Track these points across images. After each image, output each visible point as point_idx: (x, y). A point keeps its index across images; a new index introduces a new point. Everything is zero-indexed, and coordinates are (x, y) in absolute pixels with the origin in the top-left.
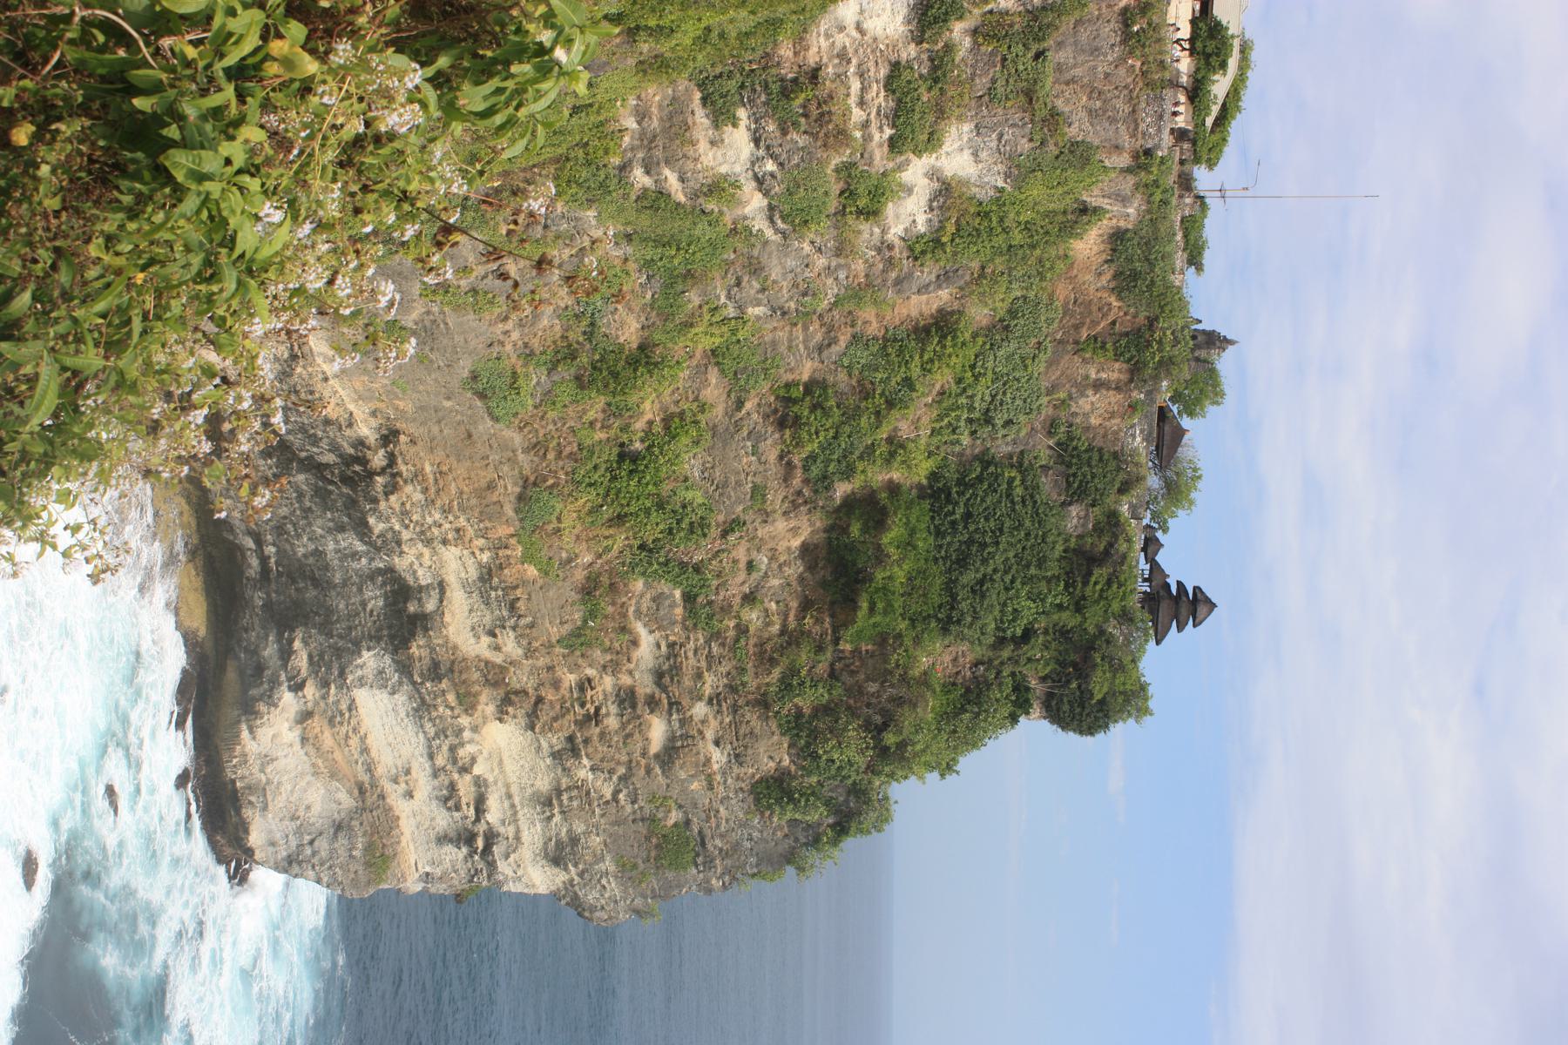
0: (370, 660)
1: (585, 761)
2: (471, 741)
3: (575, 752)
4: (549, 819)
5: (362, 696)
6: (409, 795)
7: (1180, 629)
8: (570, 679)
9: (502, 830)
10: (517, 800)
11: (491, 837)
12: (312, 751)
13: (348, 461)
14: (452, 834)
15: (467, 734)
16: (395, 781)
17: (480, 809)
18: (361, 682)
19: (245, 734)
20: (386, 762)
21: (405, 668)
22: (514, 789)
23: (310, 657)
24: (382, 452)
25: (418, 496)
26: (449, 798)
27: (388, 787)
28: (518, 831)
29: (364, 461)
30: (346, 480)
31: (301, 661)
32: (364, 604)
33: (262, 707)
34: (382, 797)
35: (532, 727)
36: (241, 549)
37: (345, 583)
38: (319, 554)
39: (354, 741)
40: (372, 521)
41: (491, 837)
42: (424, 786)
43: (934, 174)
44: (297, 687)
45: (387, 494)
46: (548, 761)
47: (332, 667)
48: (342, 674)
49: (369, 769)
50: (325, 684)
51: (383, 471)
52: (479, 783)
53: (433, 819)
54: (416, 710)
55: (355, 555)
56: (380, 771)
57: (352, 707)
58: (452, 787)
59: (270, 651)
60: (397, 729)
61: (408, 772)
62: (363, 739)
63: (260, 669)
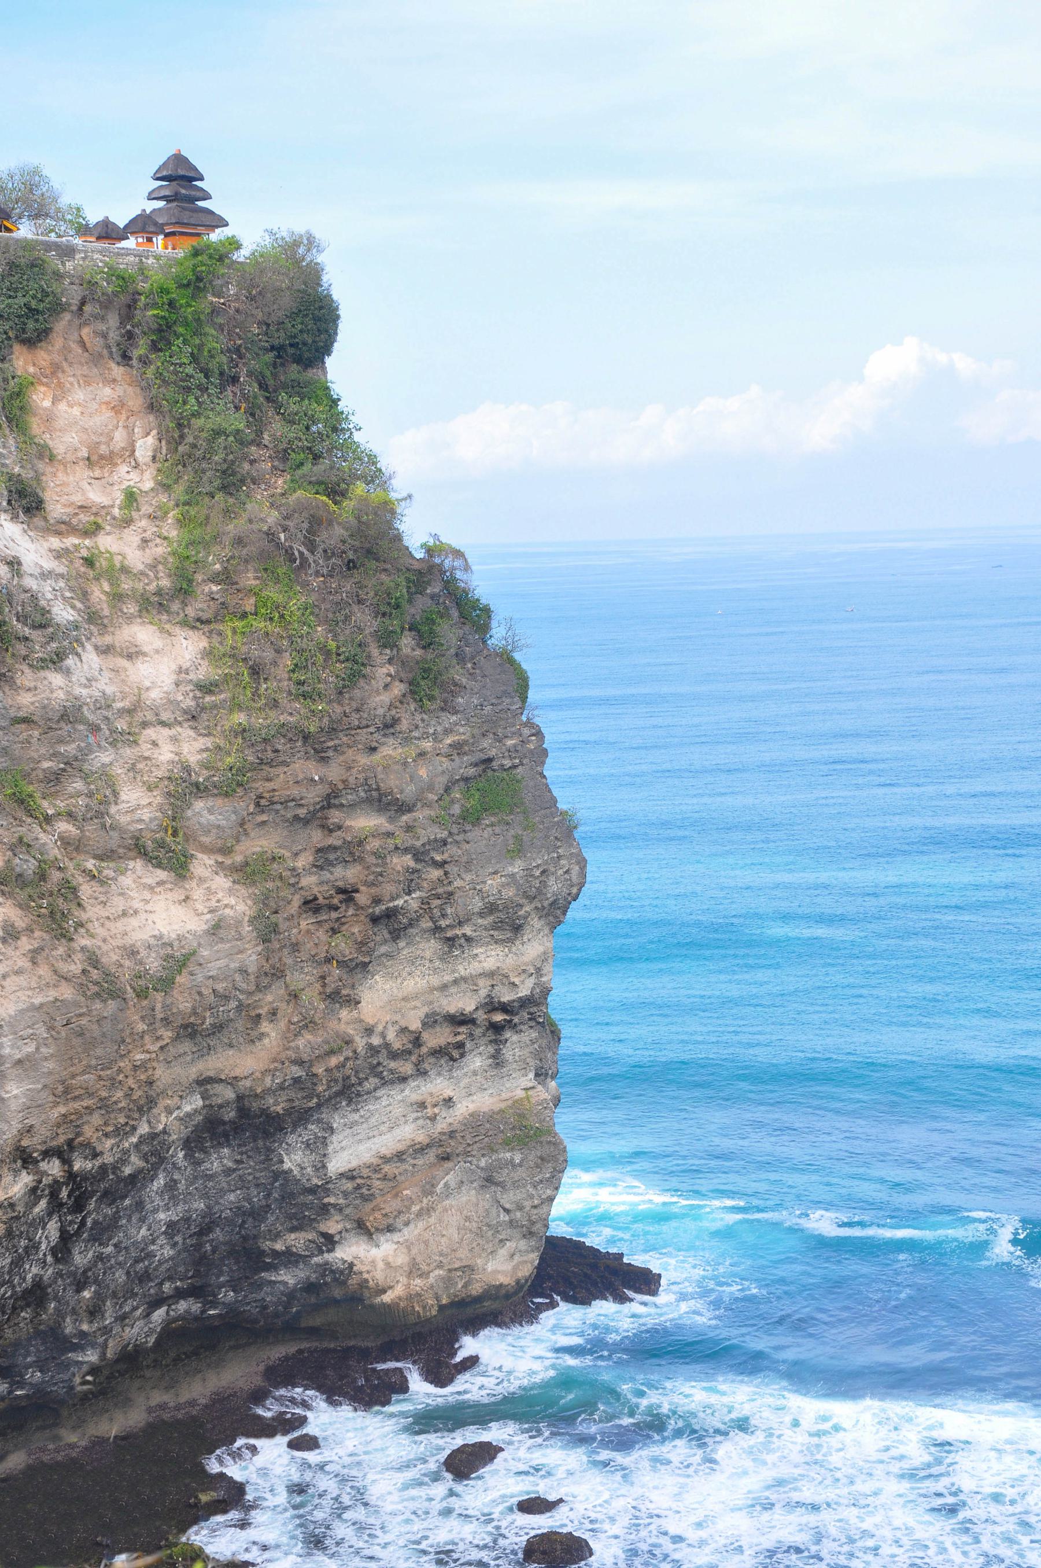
0: (294, 1159)
1: (400, 902)
2: (383, 1035)
4: (468, 939)
6: (449, 1102)
7: (207, 197)
9: (483, 993)
10: (448, 978)
12: (404, 1218)
13: (56, 1206)
14: (491, 1049)
15: (376, 1041)
16: (433, 1119)
17: (459, 1020)
19: (387, 1298)
20: (410, 1131)
21: (301, 1117)
22: (435, 981)
23: (293, 1229)
24: (43, 1166)
25: (96, 1119)
26: (450, 1055)
27: (441, 1126)
28: (483, 975)
29: (55, 1188)
30: (79, 1206)
31: (297, 1241)
32: (228, 1172)
33: (353, 1281)
34: (452, 1134)
35: (365, 965)
36: (168, 1323)
37: (205, 1196)
40: (127, 1171)
41: (492, 1006)
42: (437, 1086)
44: (330, 1242)
45: (95, 1155)
46: (402, 944)
47: (305, 1203)
48: (313, 1190)
49: (420, 1150)
50: (325, 1210)
51: (66, 1162)
52: (431, 1021)
53: (475, 1073)
54: (350, 1101)
55: (171, 1186)
56: (421, 1138)
57: (349, 1175)
58: (438, 1052)
59: (288, 1277)
60: (373, 1121)
61: (422, 1105)
62: (386, 1159)
63: (310, 1287)
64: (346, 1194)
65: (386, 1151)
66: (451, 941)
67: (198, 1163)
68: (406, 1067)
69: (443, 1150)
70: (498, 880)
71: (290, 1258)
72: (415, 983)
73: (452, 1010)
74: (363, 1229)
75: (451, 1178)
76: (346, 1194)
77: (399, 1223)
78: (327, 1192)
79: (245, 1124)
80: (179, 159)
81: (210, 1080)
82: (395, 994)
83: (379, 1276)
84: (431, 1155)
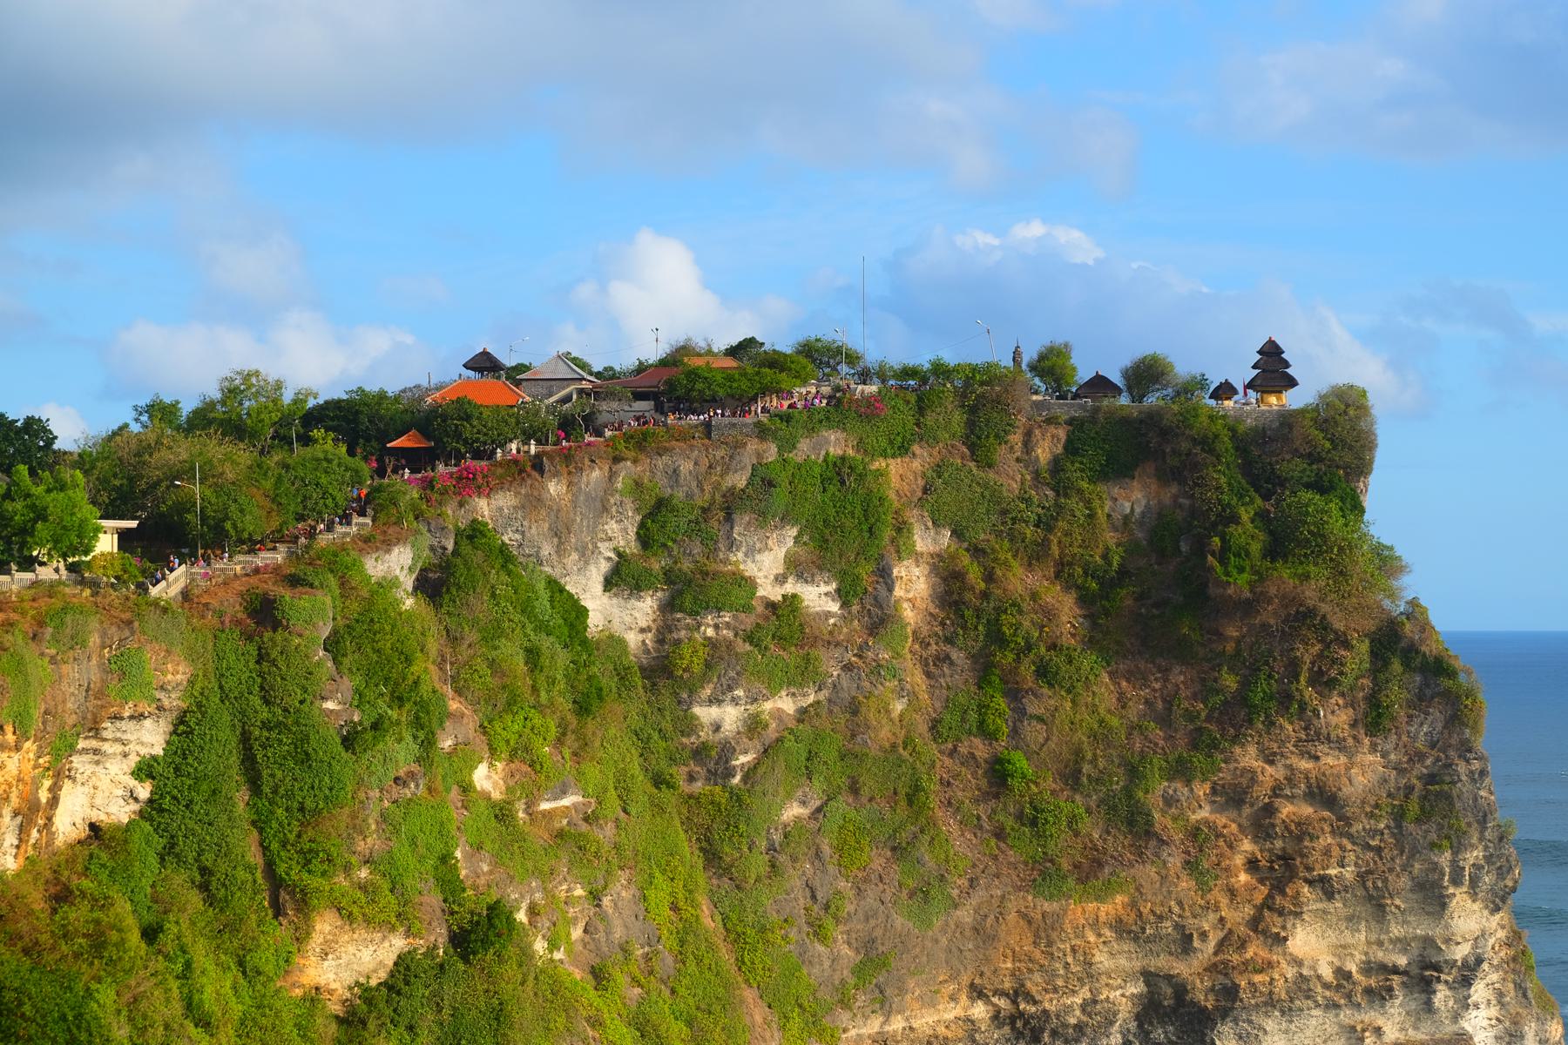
1: (1332, 872)
2: (1314, 968)
3: (1324, 880)
8: (1243, 877)
9: (1416, 952)
17: (1395, 970)
26: (1379, 996)
28: (1415, 938)
29: (1012, 1020)
40: (1073, 1021)
42: (1371, 1016)
43: (780, 580)
51: (1015, 1003)
52: (1368, 968)
54: (1283, 1013)
58: (1368, 991)
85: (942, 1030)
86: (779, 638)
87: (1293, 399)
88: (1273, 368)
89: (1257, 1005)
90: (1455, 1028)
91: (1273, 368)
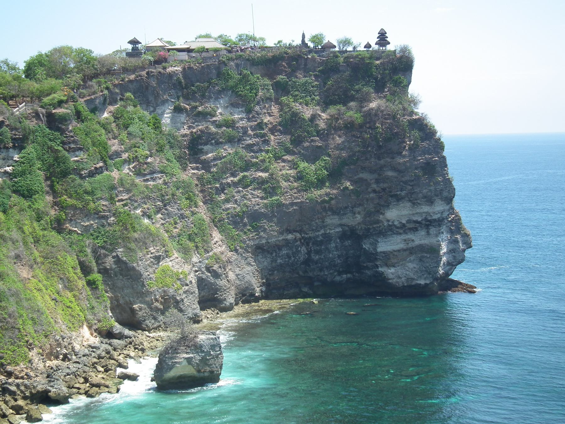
0: (366, 246)
2: (393, 222)
3: (396, 196)
4: (419, 204)
5: (379, 250)
9: (424, 217)
10: (414, 212)
11: (426, 219)
12: (397, 265)
15: (390, 223)
16: (408, 244)
18: (375, 249)
19: (390, 281)
20: (402, 246)
22: (411, 212)
29: (300, 240)
31: (371, 264)
34: (413, 248)
38: (339, 257)
39: (395, 253)
41: (426, 219)
42: (410, 236)
47: (373, 256)
49: (405, 250)
50: (376, 259)
52: (409, 221)
53: (422, 235)
56: (405, 247)
57: (384, 252)
59: (369, 272)
60: (392, 242)
61: (405, 240)
62: (394, 251)
64: (383, 257)
65: (395, 249)
66: (414, 204)
67: (343, 243)
68: (401, 231)
69: (411, 251)
70: (427, 191)
71: (367, 268)
72: (405, 212)
73: (415, 219)
74: (387, 265)
75: (412, 258)
76: (383, 257)
77: (396, 265)
78: (377, 255)
79: (351, 235)
80: (382, 29)
81: (344, 225)
82: (395, 214)
83: (391, 276)
84: (407, 252)
85: (278, 243)
86: (41, 66)
87: (390, 48)
88: (383, 39)
89: (375, 234)
90: (436, 239)
91: (383, 39)
